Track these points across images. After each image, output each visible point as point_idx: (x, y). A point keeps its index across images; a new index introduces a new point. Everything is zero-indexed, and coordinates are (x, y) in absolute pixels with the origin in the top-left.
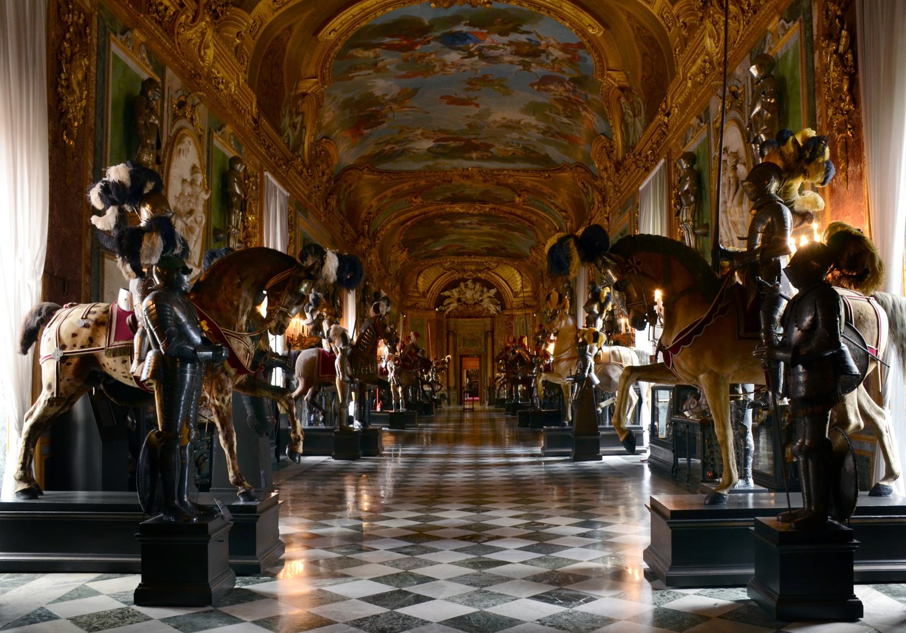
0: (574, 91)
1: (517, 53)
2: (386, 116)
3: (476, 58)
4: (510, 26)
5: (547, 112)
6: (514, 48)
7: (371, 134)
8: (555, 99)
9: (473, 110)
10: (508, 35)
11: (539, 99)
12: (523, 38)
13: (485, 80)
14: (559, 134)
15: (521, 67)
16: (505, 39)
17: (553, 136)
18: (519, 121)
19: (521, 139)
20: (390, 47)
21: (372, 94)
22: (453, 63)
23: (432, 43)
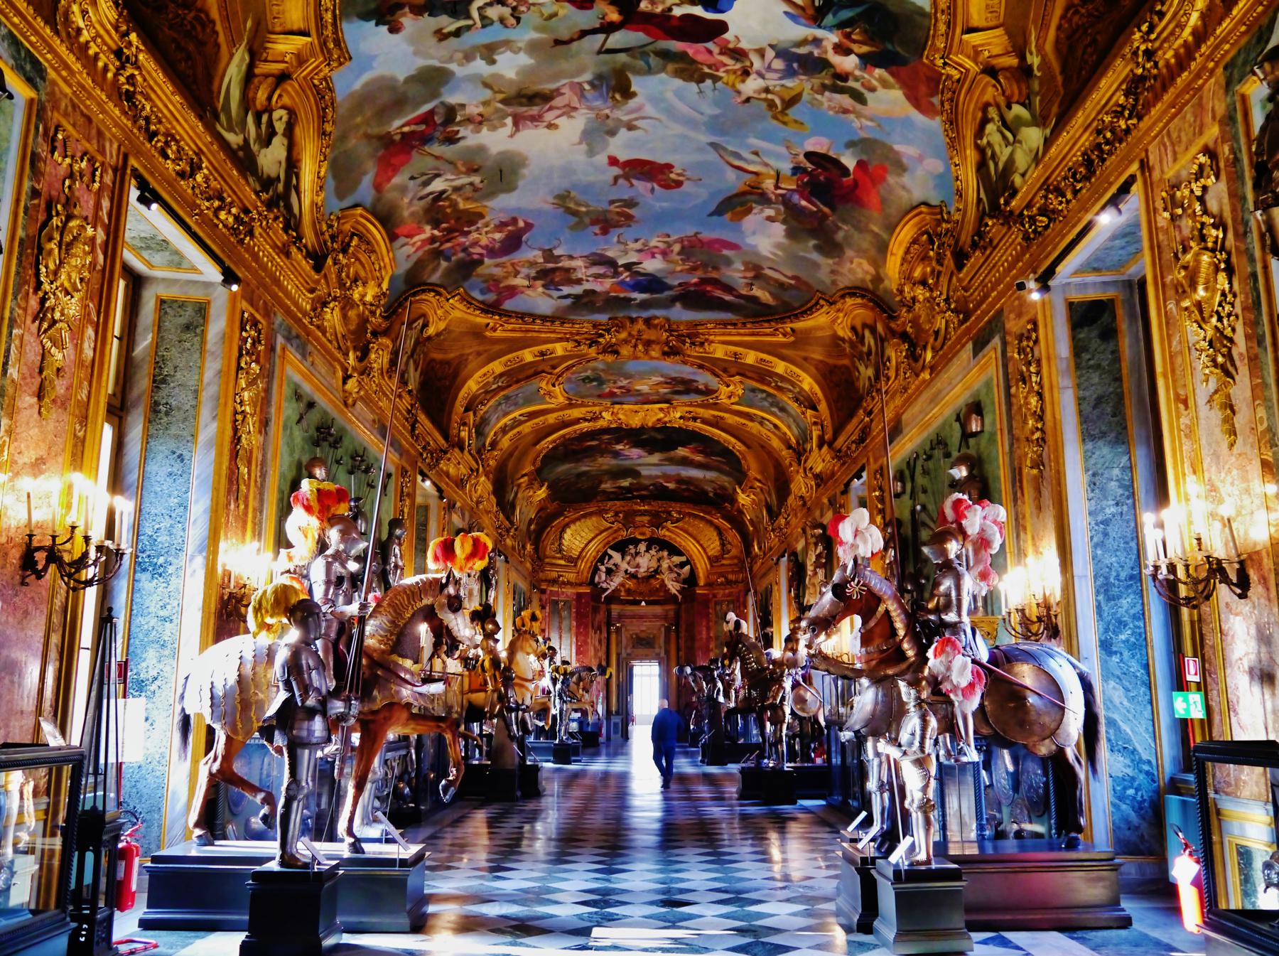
0: (465, 250)
1: (568, 270)
2: (797, 170)
3: (621, 262)
4: (585, 300)
5: (476, 179)
6: (574, 277)
7: (851, 145)
8: (482, 216)
9: (622, 146)
10: (585, 291)
11: (501, 205)
12: (566, 290)
13: (606, 224)
14: (425, 139)
15: (557, 252)
16: (587, 286)
17: (427, 118)
18: (516, 124)
19: (489, 53)
20: (729, 289)
21: (790, 234)
22: (653, 257)
23: (676, 283)
